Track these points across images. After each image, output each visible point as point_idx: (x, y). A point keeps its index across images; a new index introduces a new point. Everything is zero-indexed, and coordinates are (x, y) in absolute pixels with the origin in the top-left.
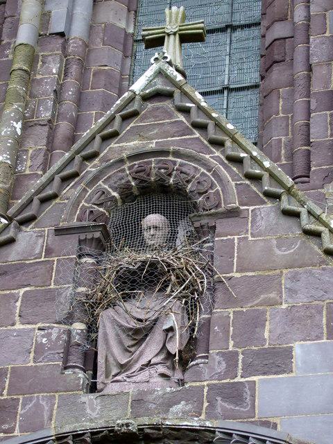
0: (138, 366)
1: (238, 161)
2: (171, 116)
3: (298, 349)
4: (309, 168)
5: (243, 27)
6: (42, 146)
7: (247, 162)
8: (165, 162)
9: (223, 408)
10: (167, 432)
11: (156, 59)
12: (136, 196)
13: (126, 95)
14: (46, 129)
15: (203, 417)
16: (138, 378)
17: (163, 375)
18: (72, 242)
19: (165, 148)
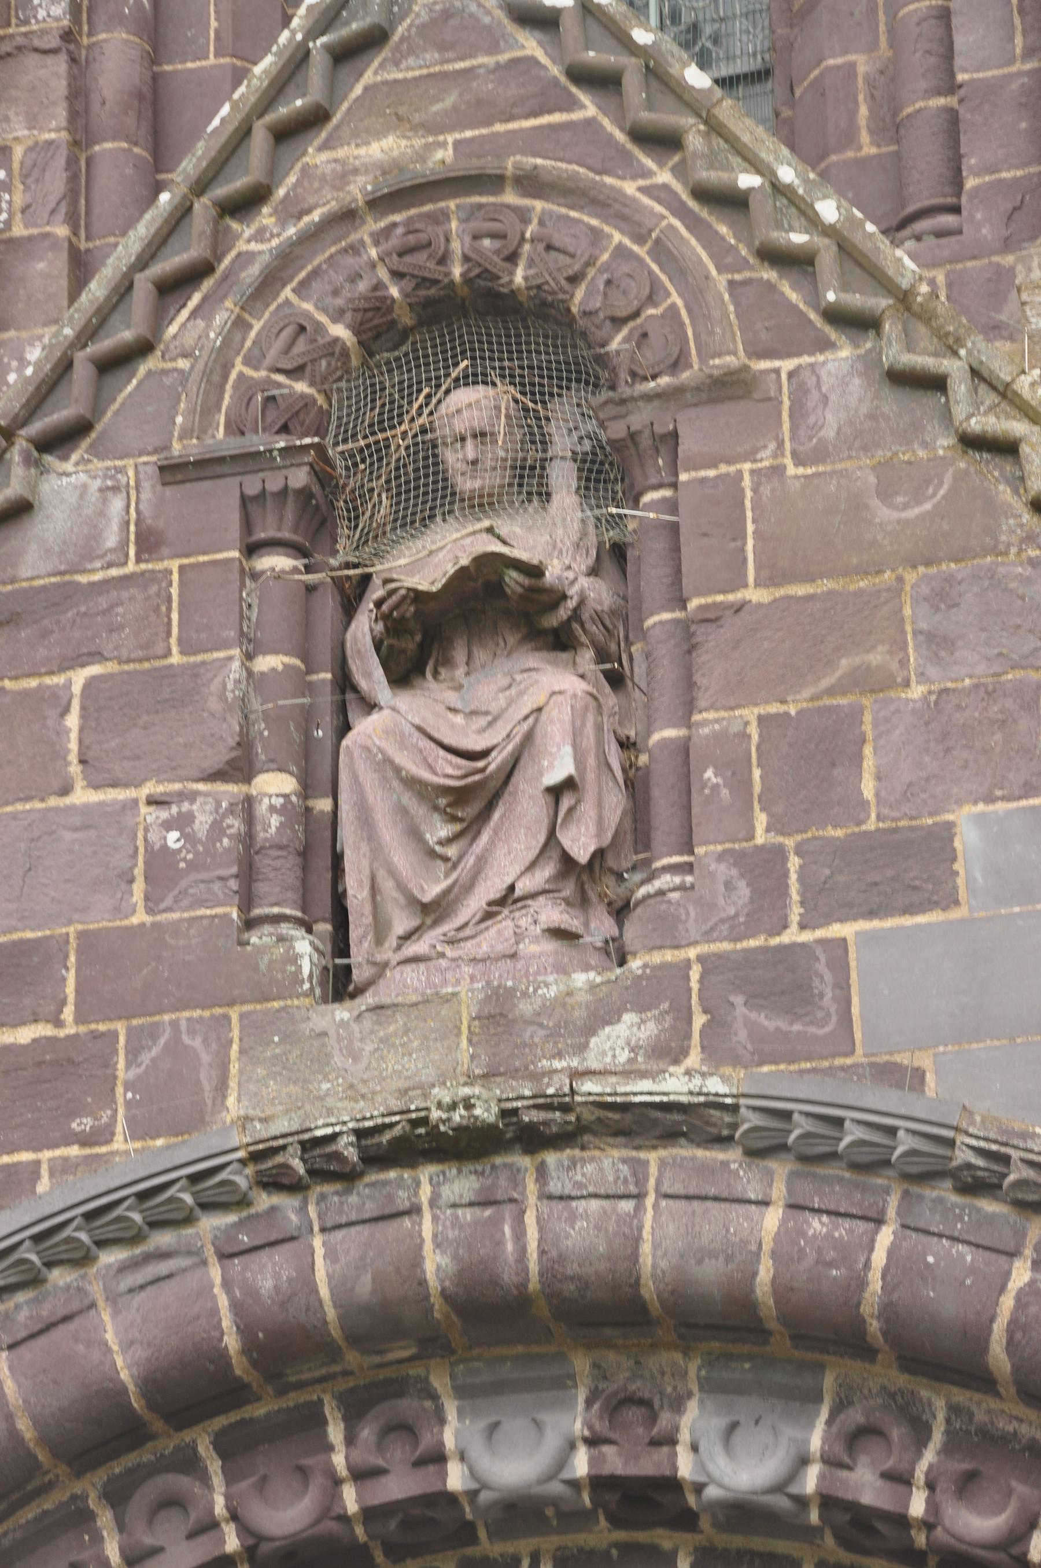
2: (494, 45)
4: (958, 183)
7: (761, 208)
8: (493, 213)
12: (405, 334)
14: (60, 65)
15: (694, 1059)
17: (559, 934)
19: (488, 165)
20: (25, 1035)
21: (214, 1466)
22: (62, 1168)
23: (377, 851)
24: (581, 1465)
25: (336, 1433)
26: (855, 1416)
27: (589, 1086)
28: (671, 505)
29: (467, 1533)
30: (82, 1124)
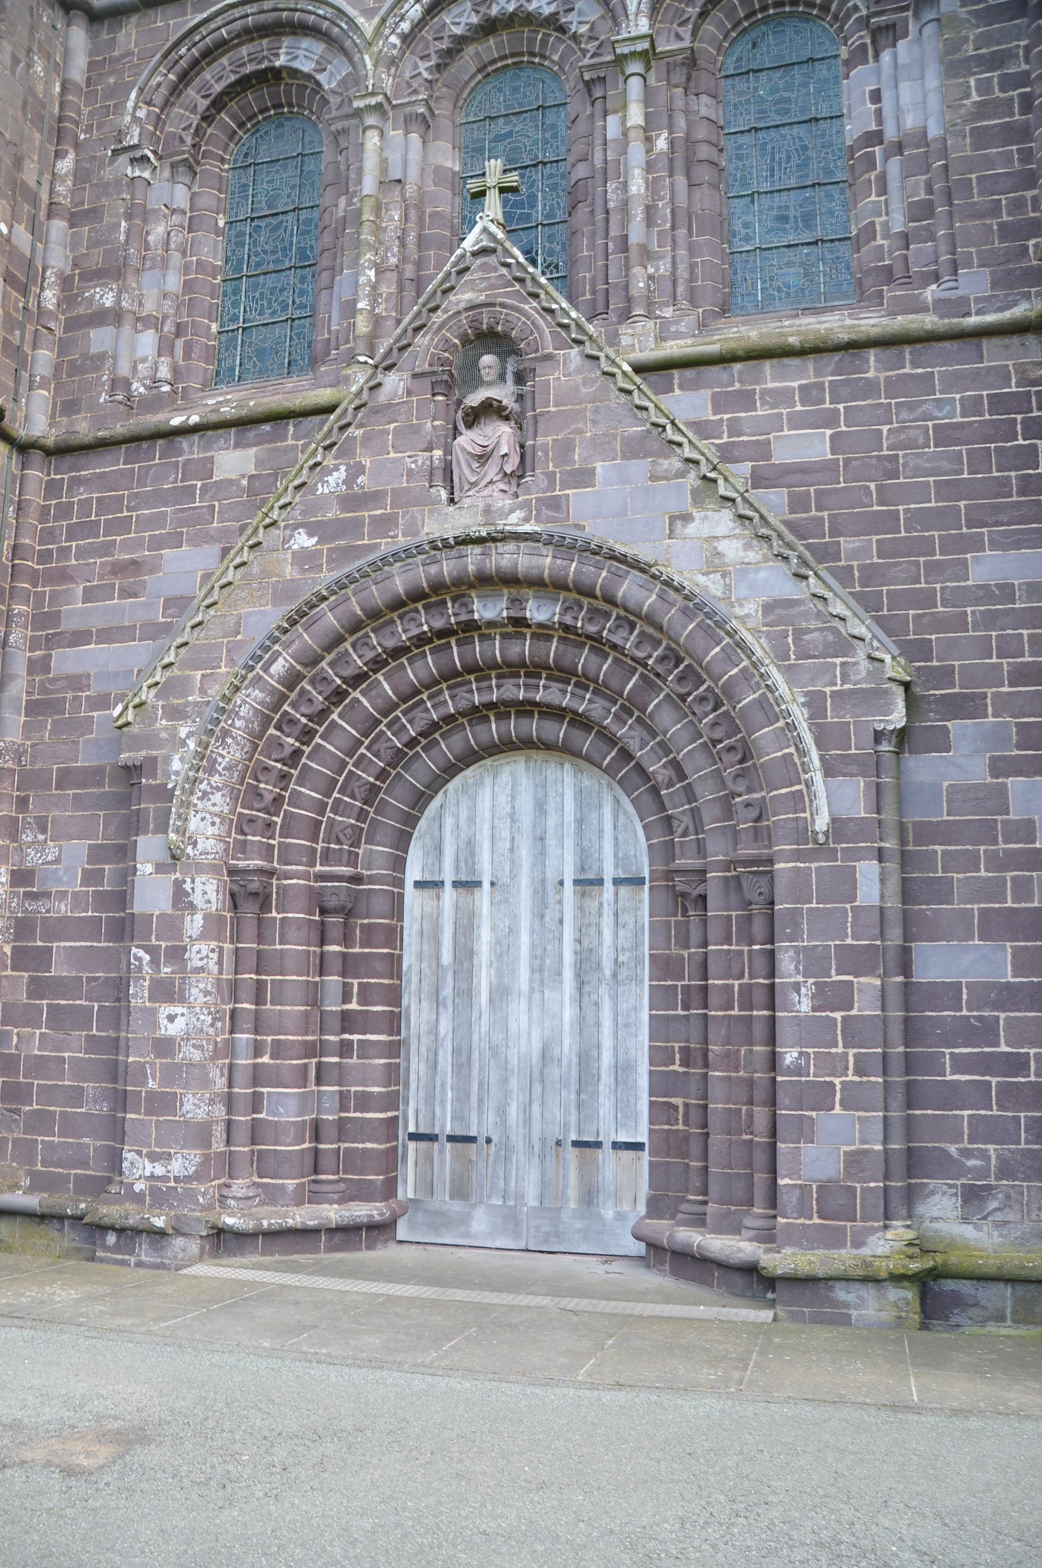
1: (551, 311)
2: (496, 270)
3: (599, 467)
6: (393, 289)
7: (559, 313)
8: (493, 312)
13: (459, 252)
14: (395, 273)
16: (485, 493)
18: (427, 383)
19: (492, 300)
20: (378, 512)
21: (422, 612)
22: (387, 543)
23: (461, 469)
24: (505, 614)
25: (450, 605)
26: (567, 605)
27: (507, 528)
28: (533, 386)
29: (479, 628)
30: (391, 533)
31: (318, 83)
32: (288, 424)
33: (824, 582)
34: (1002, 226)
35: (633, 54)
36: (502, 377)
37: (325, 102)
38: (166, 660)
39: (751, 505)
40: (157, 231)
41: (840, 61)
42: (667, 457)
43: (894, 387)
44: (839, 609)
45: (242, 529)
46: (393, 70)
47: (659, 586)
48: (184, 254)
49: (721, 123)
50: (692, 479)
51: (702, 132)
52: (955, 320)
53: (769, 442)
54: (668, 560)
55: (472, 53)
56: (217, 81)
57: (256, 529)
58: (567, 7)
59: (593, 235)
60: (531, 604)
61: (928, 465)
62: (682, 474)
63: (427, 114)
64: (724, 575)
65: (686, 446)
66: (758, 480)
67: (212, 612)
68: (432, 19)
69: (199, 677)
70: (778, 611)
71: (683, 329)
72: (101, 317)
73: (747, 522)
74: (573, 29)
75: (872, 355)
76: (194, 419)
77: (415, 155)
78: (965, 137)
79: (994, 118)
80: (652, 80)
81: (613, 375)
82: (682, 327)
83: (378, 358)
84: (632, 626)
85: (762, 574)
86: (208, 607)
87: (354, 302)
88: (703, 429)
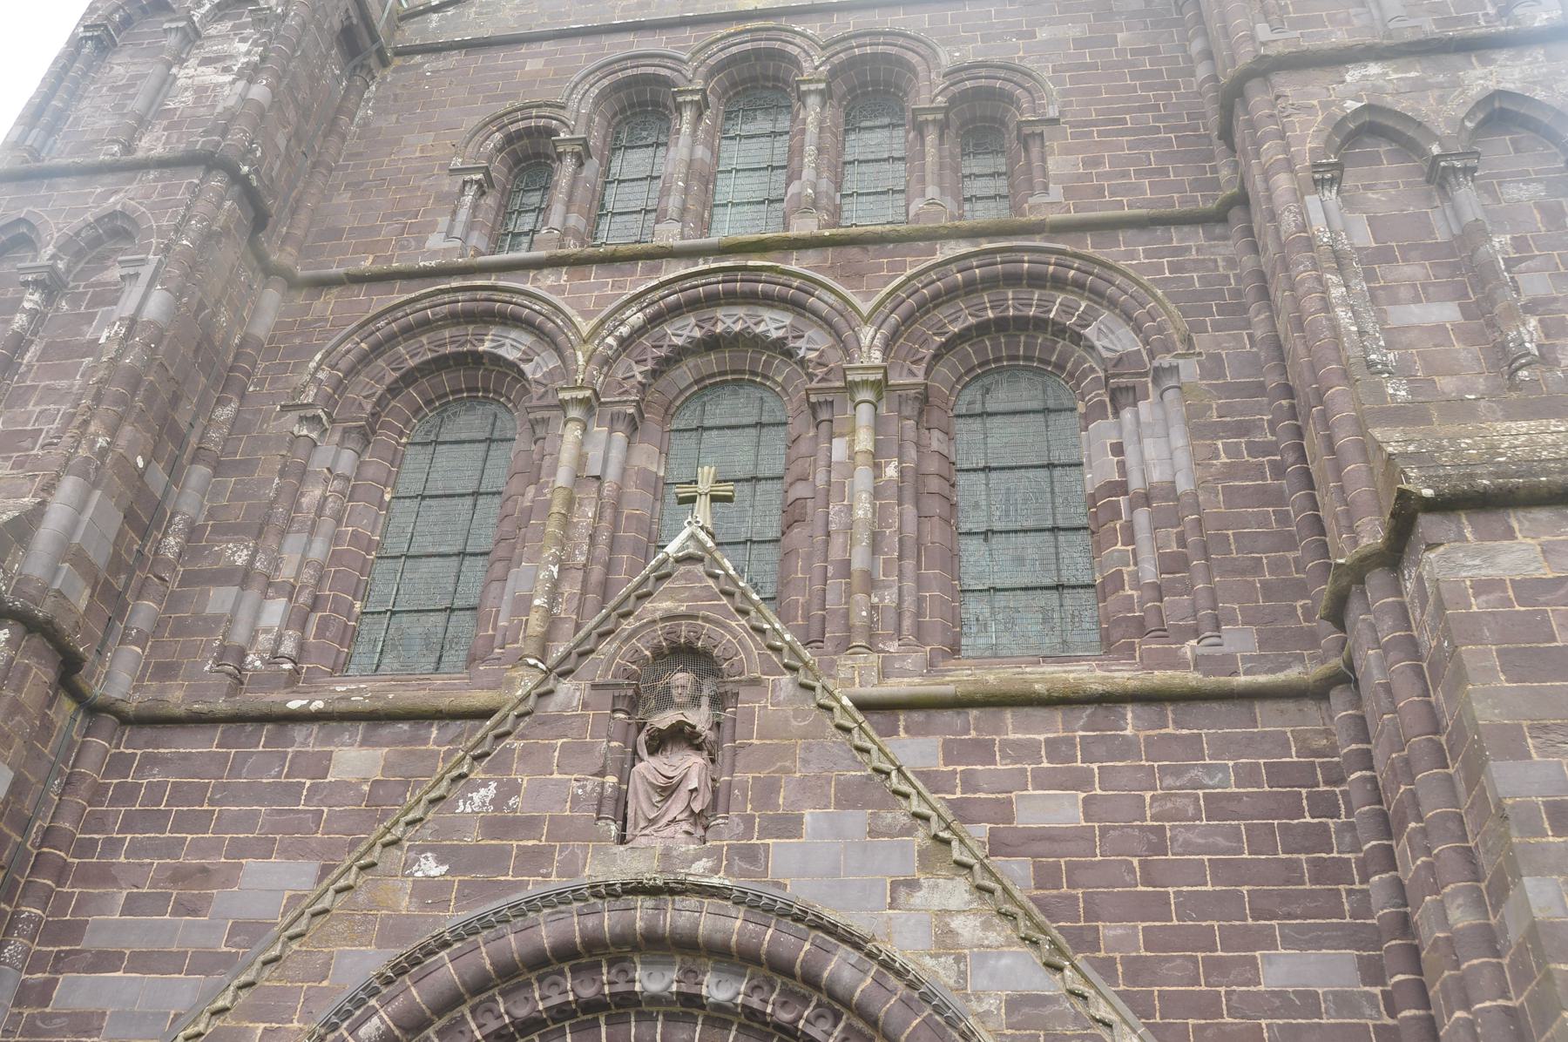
0: (664, 821)
1: (761, 631)
5: (766, 479)
6: (577, 590)
9: (740, 868)
10: (689, 887)
11: (689, 523)
13: (660, 556)
14: (581, 572)
17: (687, 833)
18: (608, 696)
19: (695, 613)
20: (530, 843)
21: (569, 975)
22: (536, 883)
23: (638, 802)
24: (674, 988)
25: (605, 970)
26: (755, 982)
27: (690, 878)
28: (735, 713)
29: (639, 1003)
30: (543, 871)
31: (522, 373)
32: (431, 725)
33: (1083, 976)
34: (1264, 584)
35: (865, 383)
36: (695, 702)
37: (526, 391)
38: (220, 1004)
39: (992, 874)
40: (312, 495)
41: (1076, 414)
42: (890, 809)
43: (1157, 747)
44: (1103, 1012)
45: (353, 845)
46: (605, 369)
47: (875, 967)
48: (339, 522)
49: (953, 459)
50: (920, 838)
51: (933, 465)
52: (1222, 678)
53: (1010, 802)
54: (888, 935)
55: (691, 365)
56: (411, 357)
57: (372, 846)
58: (796, 334)
59: (809, 557)
60: (708, 978)
61: (1201, 841)
62: (908, 831)
63: (636, 416)
64: (959, 959)
65: (914, 798)
66: (998, 846)
67: (295, 946)
68: (653, 328)
69: (259, 1032)
70: (1026, 1010)
71: (910, 667)
72: (226, 576)
73: (987, 895)
74: (801, 353)
75: (1129, 712)
76: (318, 705)
77: (616, 455)
78: (1217, 495)
79: (1247, 480)
80: (883, 410)
81: (830, 709)
82: (909, 664)
83: (551, 661)
84: (837, 1018)
85: (1005, 961)
86: (291, 938)
87: (531, 598)
88: (933, 780)
